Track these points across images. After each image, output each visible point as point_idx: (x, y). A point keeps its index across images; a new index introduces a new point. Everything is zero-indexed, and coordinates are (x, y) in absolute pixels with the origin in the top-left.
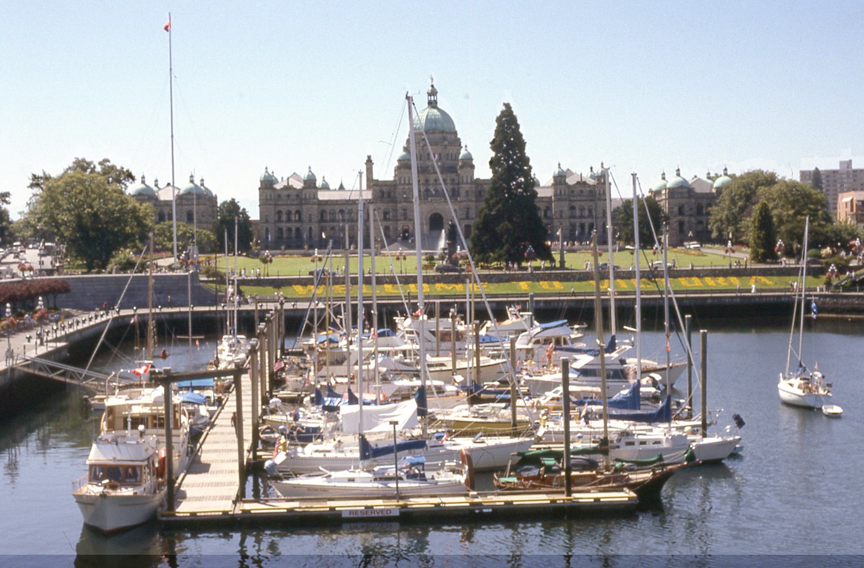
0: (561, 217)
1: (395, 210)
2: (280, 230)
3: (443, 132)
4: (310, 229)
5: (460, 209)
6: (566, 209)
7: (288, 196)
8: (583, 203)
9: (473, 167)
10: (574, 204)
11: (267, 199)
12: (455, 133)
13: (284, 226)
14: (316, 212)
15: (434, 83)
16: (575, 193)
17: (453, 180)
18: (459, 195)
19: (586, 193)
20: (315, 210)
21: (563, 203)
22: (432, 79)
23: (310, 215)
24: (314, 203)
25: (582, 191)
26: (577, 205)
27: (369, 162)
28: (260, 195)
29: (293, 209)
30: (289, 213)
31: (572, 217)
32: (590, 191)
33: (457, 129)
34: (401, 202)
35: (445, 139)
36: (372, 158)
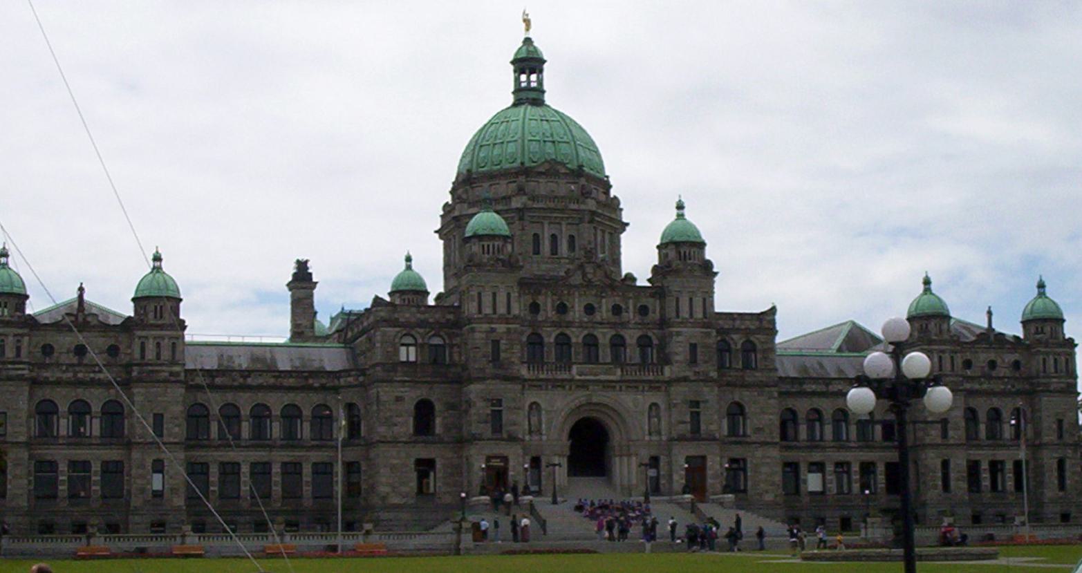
0: (945, 434)
1: (459, 408)
2: (46, 468)
3: (578, 173)
5: (670, 406)
7: (80, 350)
8: (996, 402)
10: (975, 402)
12: (607, 186)
13: (61, 455)
15: (531, 35)
17: (643, 310)
18: (666, 360)
20: (174, 402)
22: (527, 22)
24: (173, 379)
25: (992, 365)
27: (302, 279)
29: (96, 399)
30: (80, 411)
32: (1016, 365)
33: (612, 170)
35: (585, 194)
36: (313, 269)
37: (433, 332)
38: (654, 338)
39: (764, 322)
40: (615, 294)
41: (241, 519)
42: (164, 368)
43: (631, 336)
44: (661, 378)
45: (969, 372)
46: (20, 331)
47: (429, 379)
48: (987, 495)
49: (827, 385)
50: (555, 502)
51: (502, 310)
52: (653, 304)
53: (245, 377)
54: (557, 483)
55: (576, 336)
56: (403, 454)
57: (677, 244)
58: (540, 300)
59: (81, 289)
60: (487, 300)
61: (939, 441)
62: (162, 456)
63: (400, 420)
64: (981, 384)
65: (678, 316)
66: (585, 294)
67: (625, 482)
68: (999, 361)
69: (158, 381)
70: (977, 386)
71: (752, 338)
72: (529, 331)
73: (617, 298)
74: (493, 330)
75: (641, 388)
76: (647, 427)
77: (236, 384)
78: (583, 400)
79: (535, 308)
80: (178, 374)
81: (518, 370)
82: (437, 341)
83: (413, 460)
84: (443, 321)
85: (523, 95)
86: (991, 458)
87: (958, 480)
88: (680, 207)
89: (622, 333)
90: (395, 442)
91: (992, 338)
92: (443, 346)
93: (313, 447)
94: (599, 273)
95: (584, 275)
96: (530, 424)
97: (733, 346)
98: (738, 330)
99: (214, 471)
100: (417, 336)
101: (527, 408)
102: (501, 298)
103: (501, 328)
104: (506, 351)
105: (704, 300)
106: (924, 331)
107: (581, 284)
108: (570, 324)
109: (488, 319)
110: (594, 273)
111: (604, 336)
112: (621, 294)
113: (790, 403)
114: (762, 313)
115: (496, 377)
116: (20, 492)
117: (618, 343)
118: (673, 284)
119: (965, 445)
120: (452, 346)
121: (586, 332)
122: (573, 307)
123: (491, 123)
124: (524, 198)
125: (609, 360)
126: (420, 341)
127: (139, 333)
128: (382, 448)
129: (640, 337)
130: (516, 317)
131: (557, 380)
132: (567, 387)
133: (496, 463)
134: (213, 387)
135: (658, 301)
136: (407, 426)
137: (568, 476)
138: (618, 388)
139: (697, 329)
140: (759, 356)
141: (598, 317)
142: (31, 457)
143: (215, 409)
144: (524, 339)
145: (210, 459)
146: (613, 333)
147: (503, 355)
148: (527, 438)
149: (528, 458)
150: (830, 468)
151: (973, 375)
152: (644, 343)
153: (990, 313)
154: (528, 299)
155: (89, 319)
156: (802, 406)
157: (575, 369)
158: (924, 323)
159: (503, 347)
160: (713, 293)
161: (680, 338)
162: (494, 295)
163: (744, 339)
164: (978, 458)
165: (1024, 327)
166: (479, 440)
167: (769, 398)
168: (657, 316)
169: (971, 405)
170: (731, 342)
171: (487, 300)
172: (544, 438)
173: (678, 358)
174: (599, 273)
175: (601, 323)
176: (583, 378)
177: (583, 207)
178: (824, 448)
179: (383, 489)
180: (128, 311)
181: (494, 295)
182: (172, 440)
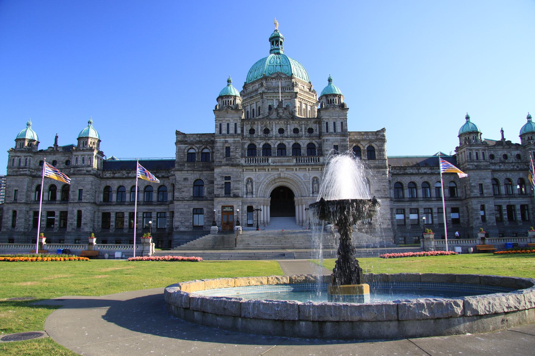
4: (80, 212)
6: (488, 182)
8: (509, 175)
9: (342, 107)
10: (497, 175)
11: (19, 168)
14: (89, 187)
16: (496, 160)
17: (310, 131)
19: (511, 159)
21: (483, 173)
23: (81, 191)
25: (505, 157)
26: (501, 177)
28: (11, 160)
31: (497, 195)
32: (518, 156)
34: (220, 166)
37: (203, 147)
38: (316, 144)
39: (379, 136)
40: (294, 122)
41: (123, 238)
42: (84, 169)
43: (304, 143)
44: (318, 163)
45: (493, 161)
46: (27, 155)
47: (201, 169)
48: (507, 223)
49: (418, 170)
50: (257, 230)
51: (232, 131)
52: (315, 127)
53: (128, 173)
54: (262, 219)
55: (274, 144)
56: (187, 207)
57: (326, 96)
58: (255, 127)
59: (57, 137)
60: (224, 127)
61: (479, 195)
62: (81, 209)
63: (185, 189)
64: (500, 166)
65: (327, 131)
66: (278, 123)
67: (301, 219)
68: (509, 154)
69: (81, 175)
70: (497, 167)
71: (373, 145)
72: (249, 143)
73: (296, 125)
74: (226, 142)
75: (307, 169)
76: (311, 189)
77: (124, 176)
78: (276, 176)
79: (252, 131)
80: (90, 171)
81: (239, 161)
82: (206, 151)
83: (192, 209)
84: (209, 141)
85: (273, 51)
86: (508, 204)
87: (490, 214)
88: (330, 80)
89: (299, 142)
90: (183, 200)
91: (504, 144)
92: (208, 153)
93: (157, 205)
94: (286, 113)
95: (278, 114)
96: (247, 189)
97: (362, 148)
98: (363, 140)
99: (113, 215)
100: (196, 148)
101: (245, 179)
102: (232, 127)
103: (230, 140)
104: (233, 152)
105: (342, 123)
106: (468, 140)
107: (277, 119)
108: (270, 138)
109: (225, 136)
110: (283, 113)
111: (289, 143)
112: (297, 122)
113: (399, 179)
114: (377, 131)
115: (227, 165)
116: (20, 225)
117: (296, 148)
118: (325, 116)
119: (492, 197)
120: (213, 152)
121: (279, 142)
122: (272, 130)
123: (257, 63)
124: (263, 89)
125: (291, 155)
126: (197, 151)
127: (75, 153)
128: (176, 203)
129: (310, 143)
130: (239, 135)
131: (261, 166)
132: (267, 170)
133: (228, 209)
134: (113, 178)
135: (318, 126)
136: (189, 192)
137: (271, 216)
138: (295, 169)
139: (337, 138)
140: (376, 153)
141: (286, 135)
142: (31, 209)
143: (115, 188)
144: (246, 146)
145: (112, 210)
146: (294, 142)
147: (231, 154)
148: (245, 196)
149: (245, 208)
150: (421, 211)
151: (496, 162)
152: (311, 148)
153: (502, 131)
154: (247, 128)
155: (58, 149)
156: (406, 180)
157: (270, 160)
158: (467, 136)
159: (231, 150)
160: (346, 119)
161: (329, 143)
162: (228, 125)
163: (368, 145)
164: (500, 204)
165: (521, 139)
166: (219, 197)
167: (383, 174)
168: (318, 133)
169: (495, 177)
170: (361, 146)
171: (224, 127)
172: (254, 196)
173: (326, 153)
174: (286, 113)
175: (287, 137)
176: (275, 164)
177: (292, 91)
178: (418, 201)
179: (176, 224)
180: (76, 143)
181: (228, 125)
182: (86, 201)
